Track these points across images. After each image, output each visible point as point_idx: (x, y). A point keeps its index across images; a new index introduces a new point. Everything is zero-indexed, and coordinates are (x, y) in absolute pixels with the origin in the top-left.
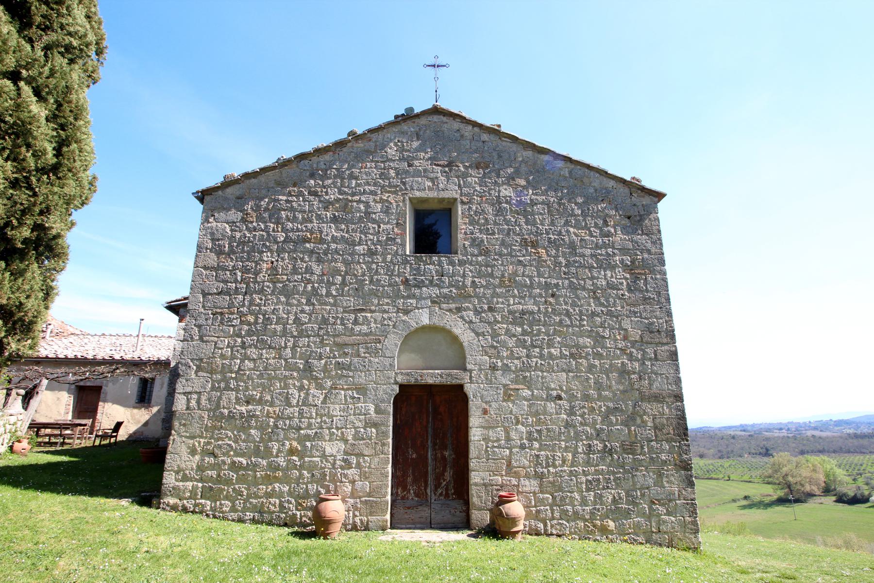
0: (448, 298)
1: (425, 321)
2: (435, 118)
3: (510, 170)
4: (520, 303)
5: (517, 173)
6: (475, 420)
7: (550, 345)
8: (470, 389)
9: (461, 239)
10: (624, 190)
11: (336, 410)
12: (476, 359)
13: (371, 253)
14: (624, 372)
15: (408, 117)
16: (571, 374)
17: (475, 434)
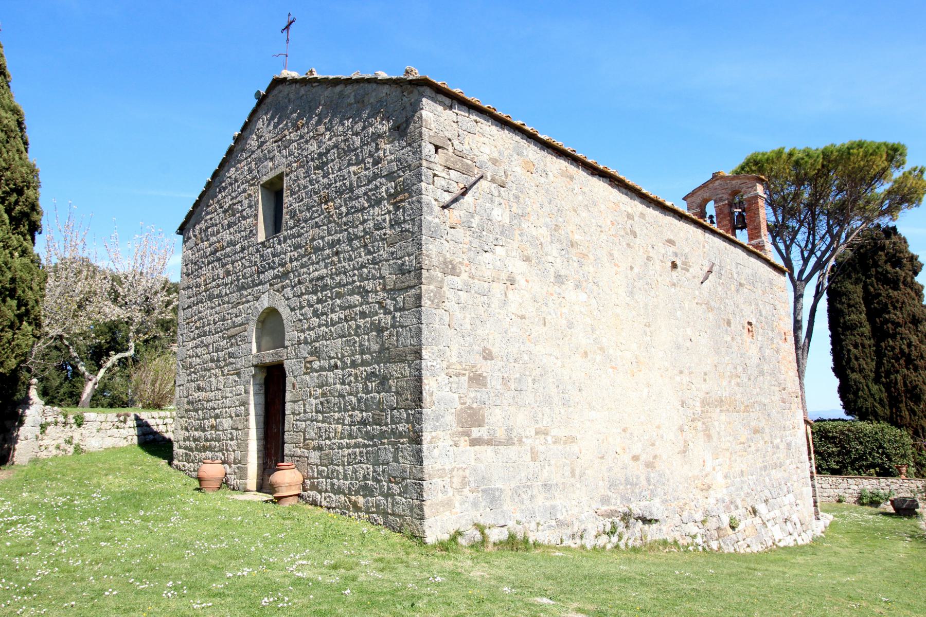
4: (316, 270)
8: (287, 365)
10: (395, 92)
12: (291, 334)
15: (262, 100)
16: (344, 339)
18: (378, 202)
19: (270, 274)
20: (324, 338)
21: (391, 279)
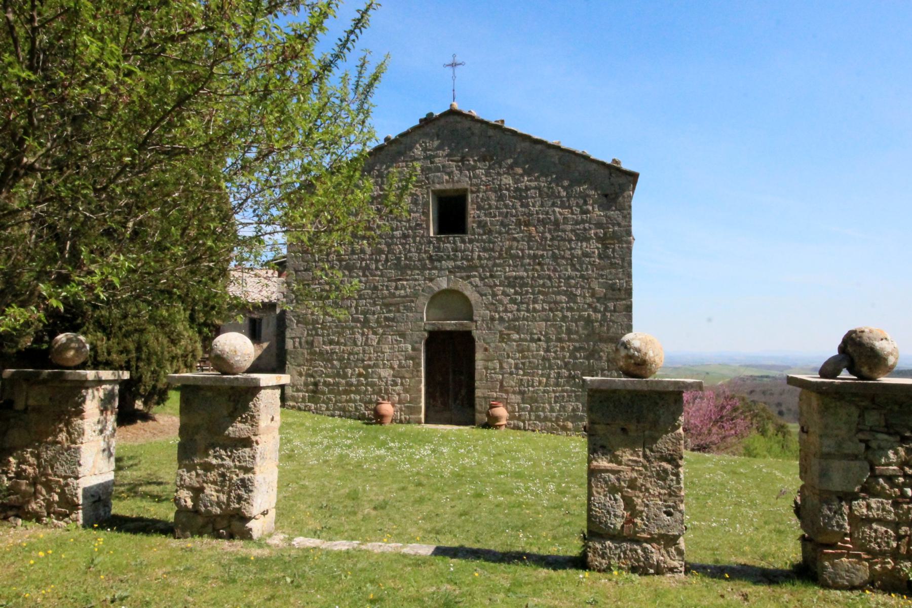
0: (460, 268)
1: (444, 285)
2: (451, 119)
3: (510, 161)
4: (514, 271)
5: (516, 164)
6: (479, 355)
7: (535, 301)
8: (476, 334)
9: (471, 223)
11: (386, 348)
12: (480, 313)
13: (405, 236)
14: (589, 321)
15: (428, 120)
16: (549, 323)
17: (479, 365)
18: (587, 239)
19: (451, 264)
20: (524, 319)
21: (600, 291)
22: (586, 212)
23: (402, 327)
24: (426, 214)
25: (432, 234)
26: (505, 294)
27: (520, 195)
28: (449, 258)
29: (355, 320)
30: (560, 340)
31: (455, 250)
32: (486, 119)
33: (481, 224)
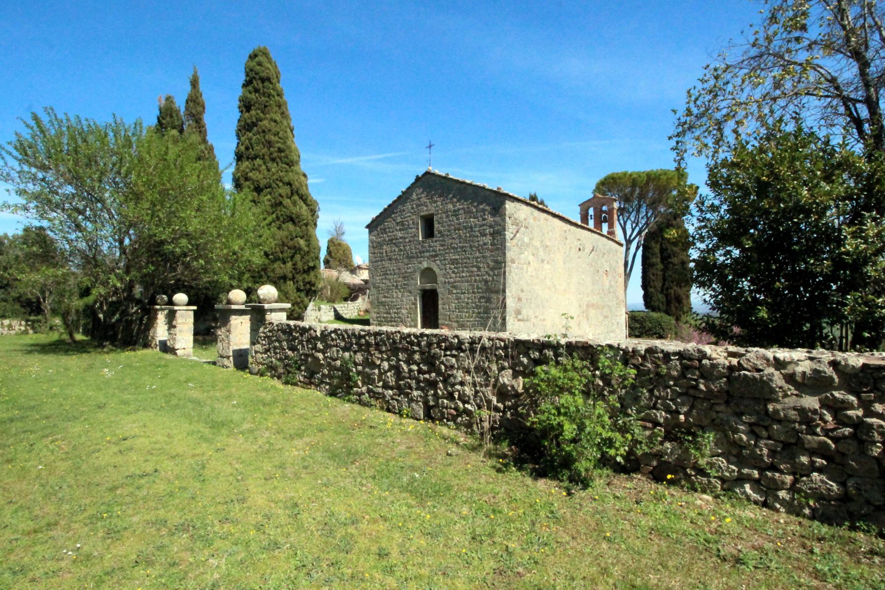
0: (432, 256)
1: (426, 266)
2: (427, 176)
3: (451, 196)
5: (454, 197)
6: (440, 302)
7: (463, 272)
8: (439, 290)
9: (436, 233)
10: (493, 195)
11: (404, 299)
12: (440, 279)
13: (410, 241)
14: (486, 282)
15: (418, 179)
17: (440, 307)
18: (485, 235)
19: (427, 254)
20: (459, 281)
21: (492, 264)
22: (484, 219)
23: (410, 288)
24: (418, 229)
25: (421, 239)
26: (450, 269)
27: (456, 213)
28: (428, 251)
29: (393, 285)
30: (474, 293)
31: (430, 246)
32: (408, 184)
33: (440, 232)
